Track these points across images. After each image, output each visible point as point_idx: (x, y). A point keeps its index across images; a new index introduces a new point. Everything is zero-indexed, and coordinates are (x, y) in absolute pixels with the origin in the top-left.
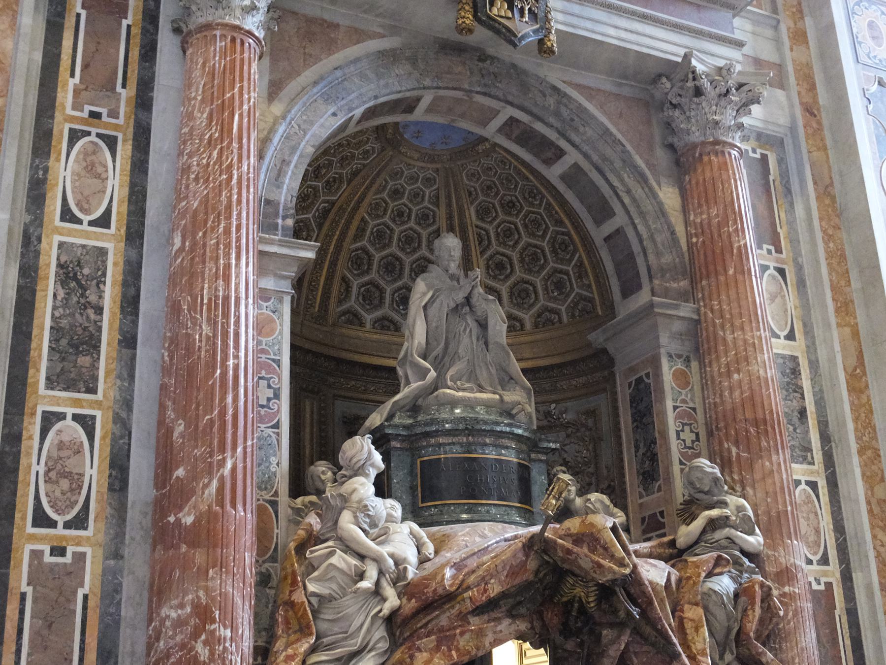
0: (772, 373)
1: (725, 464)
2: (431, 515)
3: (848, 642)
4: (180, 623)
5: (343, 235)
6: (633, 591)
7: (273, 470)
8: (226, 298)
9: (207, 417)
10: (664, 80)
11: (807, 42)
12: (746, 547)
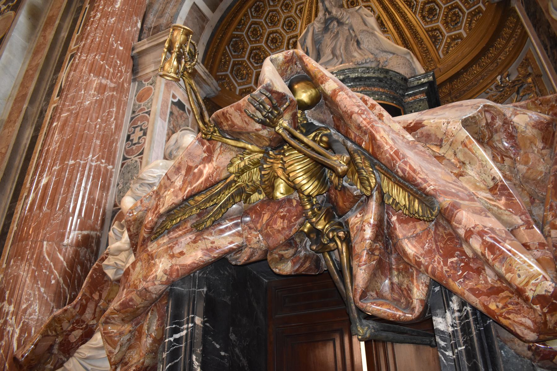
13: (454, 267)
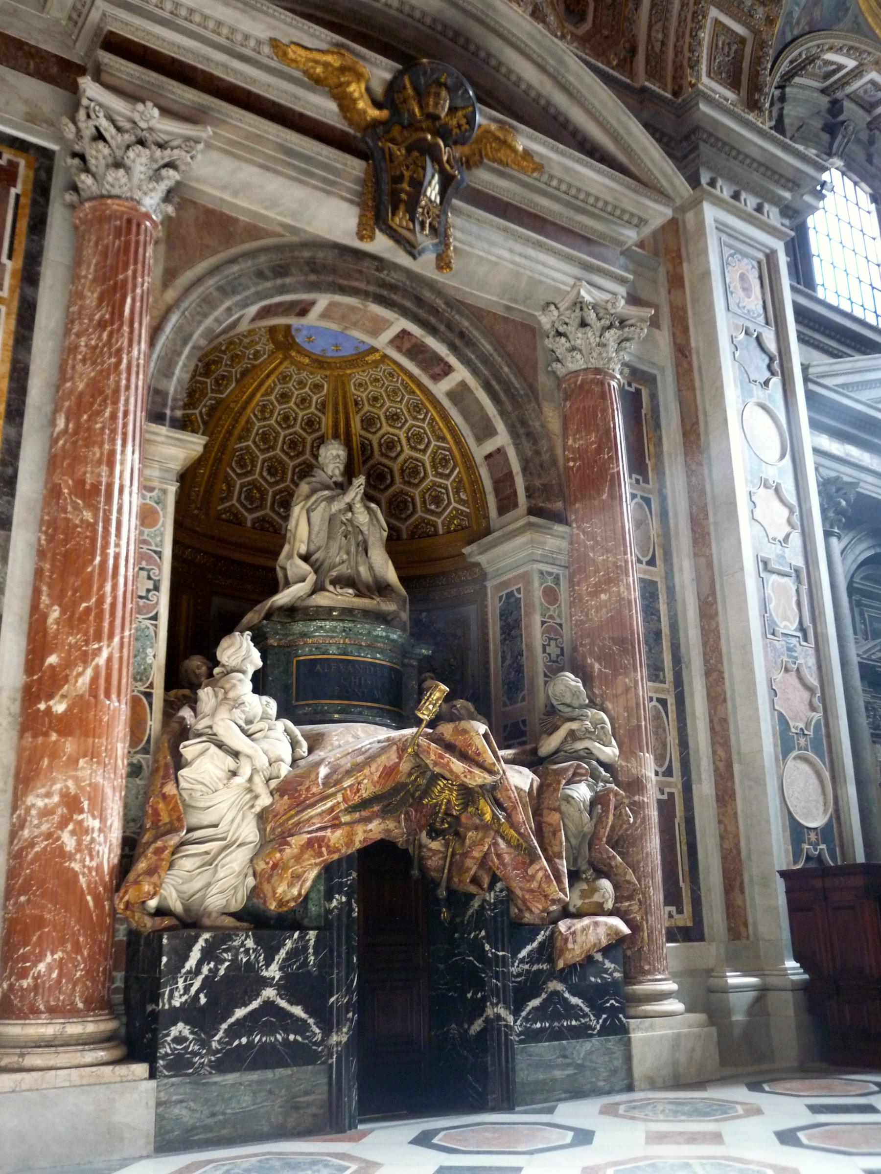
0: (635, 595)
1: (587, 679)
2: (306, 714)
3: (685, 848)
4: (46, 813)
5: (229, 433)
6: (499, 796)
7: (149, 661)
8: (110, 486)
9: (84, 605)
10: (552, 307)
11: (682, 286)
12: (602, 758)
13: (517, 875)
